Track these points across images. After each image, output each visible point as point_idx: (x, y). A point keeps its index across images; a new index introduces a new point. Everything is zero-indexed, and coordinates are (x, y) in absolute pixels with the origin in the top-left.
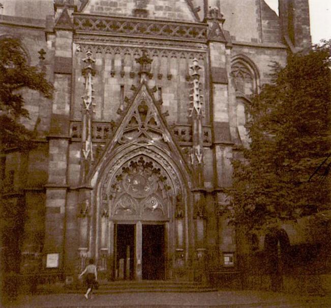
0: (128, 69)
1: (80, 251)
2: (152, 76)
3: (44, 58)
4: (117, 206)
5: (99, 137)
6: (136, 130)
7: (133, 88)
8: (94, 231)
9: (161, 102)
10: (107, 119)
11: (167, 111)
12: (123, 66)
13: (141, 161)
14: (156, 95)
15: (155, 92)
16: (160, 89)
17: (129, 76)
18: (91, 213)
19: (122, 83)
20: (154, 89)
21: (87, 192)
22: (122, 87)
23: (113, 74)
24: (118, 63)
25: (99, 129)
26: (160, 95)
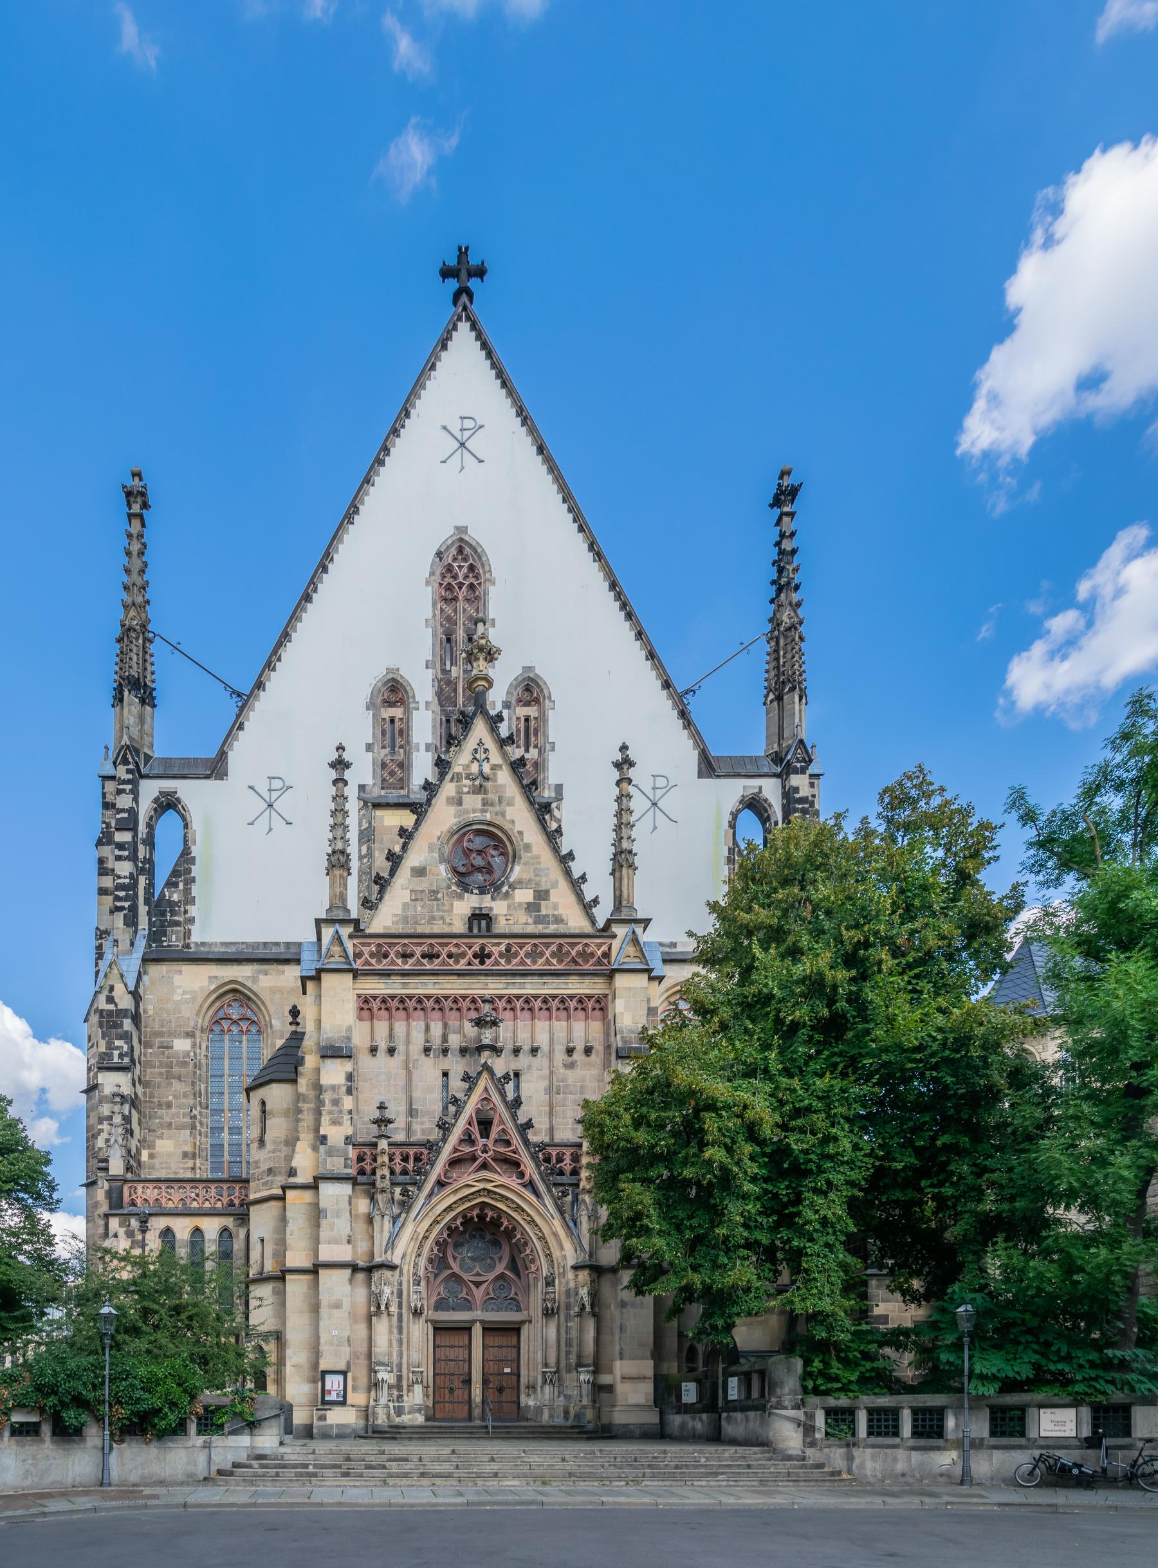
0: (455, 1041)
2: (501, 1051)
3: (298, 1024)
6: (474, 1158)
8: (400, 1342)
9: (517, 1102)
10: (418, 1137)
11: (530, 1120)
12: (445, 1038)
14: (510, 1087)
17: (457, 1052)
18: (394, 1309)
19: (446, 1067)
20: (506, 1077)
21: (387, 1273)
22: (445, 1074)
23: (427, 1050)
24: (437, 1029)
25: (405, 1159)
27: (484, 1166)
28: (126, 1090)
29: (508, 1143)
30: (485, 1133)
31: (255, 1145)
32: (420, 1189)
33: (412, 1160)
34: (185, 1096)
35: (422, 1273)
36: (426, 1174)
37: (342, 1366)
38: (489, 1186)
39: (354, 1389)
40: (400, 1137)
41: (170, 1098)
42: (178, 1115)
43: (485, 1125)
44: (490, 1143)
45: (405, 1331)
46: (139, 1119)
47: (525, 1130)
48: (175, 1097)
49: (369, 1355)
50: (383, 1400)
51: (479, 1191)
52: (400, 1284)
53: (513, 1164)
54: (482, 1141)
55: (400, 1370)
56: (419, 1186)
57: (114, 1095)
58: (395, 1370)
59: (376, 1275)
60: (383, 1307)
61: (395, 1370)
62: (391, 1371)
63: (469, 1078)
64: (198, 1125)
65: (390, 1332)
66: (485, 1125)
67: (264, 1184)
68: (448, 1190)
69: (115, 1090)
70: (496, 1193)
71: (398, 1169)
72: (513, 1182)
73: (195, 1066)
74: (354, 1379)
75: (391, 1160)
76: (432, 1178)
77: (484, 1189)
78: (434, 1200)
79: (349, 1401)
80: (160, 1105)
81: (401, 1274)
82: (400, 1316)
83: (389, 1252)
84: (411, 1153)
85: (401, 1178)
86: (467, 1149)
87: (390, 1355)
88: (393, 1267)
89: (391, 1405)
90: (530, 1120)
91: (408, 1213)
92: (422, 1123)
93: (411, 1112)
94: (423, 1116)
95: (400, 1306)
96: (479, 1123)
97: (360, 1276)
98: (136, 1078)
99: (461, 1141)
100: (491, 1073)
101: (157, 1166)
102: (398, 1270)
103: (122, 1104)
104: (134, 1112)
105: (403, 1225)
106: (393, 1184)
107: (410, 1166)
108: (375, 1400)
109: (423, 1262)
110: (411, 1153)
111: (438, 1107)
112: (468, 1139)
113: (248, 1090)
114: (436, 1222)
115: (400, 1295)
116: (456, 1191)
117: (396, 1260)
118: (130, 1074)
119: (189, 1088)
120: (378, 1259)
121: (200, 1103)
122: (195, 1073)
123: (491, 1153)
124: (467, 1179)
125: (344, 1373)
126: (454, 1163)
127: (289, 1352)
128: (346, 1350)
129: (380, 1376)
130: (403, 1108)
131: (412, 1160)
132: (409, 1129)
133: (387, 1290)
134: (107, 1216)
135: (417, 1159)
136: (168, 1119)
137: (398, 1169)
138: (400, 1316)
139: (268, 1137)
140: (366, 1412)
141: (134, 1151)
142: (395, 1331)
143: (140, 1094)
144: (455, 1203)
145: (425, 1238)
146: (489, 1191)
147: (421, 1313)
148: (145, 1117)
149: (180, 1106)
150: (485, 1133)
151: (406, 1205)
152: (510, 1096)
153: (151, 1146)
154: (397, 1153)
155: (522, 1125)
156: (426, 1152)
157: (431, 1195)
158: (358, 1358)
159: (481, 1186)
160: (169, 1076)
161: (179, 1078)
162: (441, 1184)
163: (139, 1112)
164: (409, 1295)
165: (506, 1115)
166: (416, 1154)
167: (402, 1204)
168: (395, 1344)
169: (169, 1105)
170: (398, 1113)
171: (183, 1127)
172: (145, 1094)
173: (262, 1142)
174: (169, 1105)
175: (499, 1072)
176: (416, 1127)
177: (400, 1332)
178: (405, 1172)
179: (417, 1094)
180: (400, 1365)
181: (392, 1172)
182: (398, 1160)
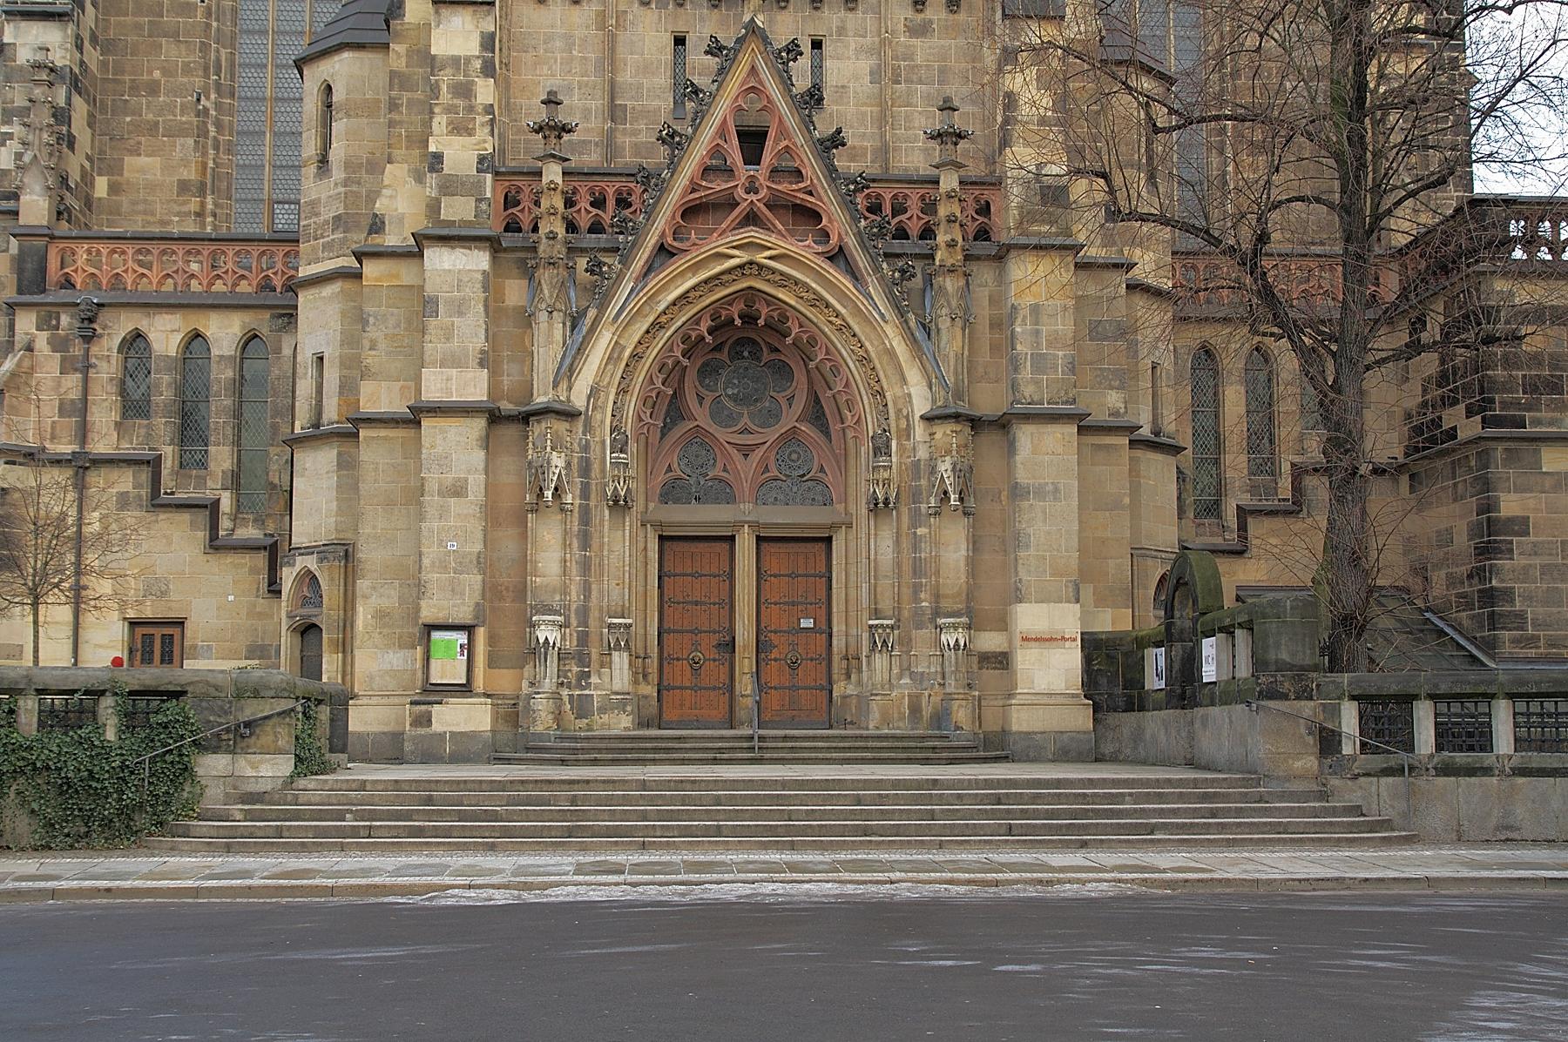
1: (533, 626)
4: (669, 469)
5: (596, 228)
7: (715, 49)
8: (585, 566)
9: (814, 98)
10: (627, 160)
13: (749, 319)
15: (795, 60)
16: (817, 45)
19: (681, 27)
20: (793, 50)
21: (561, 426)
22: (680, 41)
25: (599, 203)
26: (817, 68)
27: (751, 219)
28: (61, 57)
29: (798, 174)
30: (752, 157)
31: (312, 169)
32: (626, 262)
33: (611, 203)
34: (187, 70)
35: (629, 426)
36: (638, 232)
37: (464, 615)
38: (761, 257)
39: (492, 663)
40: (592, 159)
41: (157, 74)
42: (171, 108)
43: (752, 140)
44: (761, 172)
45: (595, 543)
46: (91, 116)
47: (827, 150)
48: (165, 72)
49: (521, 591)
50: (548, 684)
51: (741, 267)
52: (586, 448)
53: (805, 216)
54: (743, 172)
55: (584, 622)
56: (625, 255)
57: (38, 66)
58: (574, 622)
59: (537, 429)
60: (549, 494)
61: (574, 622)
62: (566, 625)
63: (721, 48)
64: (212, 128)
65: (565, 545)
66: (752, 140)
67: (328, 247)
68: (680, 263)
69: (40, 57)
70: (774, 271)
71: (584, 222)
72: (805, 249)
73: (209, 14)
74: (492, 640)
75: (569, 203)
76: (651, 241)
77: (751, 263)
78: (654, 282)
79: (479, 684)
80: (134, 89)
81: (588, 428)
82: (585, 514)
83: (564, 385)
84: (611, 191)
85: (591, 240)
86: (719, 185)
87: (565, 591)
88: (570, 415)
89: (565, 692)
90: (839, 131)
91: (602, 308)
92: (635, 133)
93: (615, 112)
94: (635, 120)
95: (585, 493)
96: (741, 135)
97: (510, 432)
98: (86, 36)
99: (707, 171)
100: (766, 41)
101: (125, 207)
102: (583, 416)
103: (51, 84)
104: (77, 100)
105: (592, 329)
106: (572, 250)
107: (606, 217)
108: (532, 684)
109: (631, 405)
110: (611, 191)
111: (665, 103)
112: (715, 168)
113: (300, 64)
114: (657, 326)
115: (585, 470)
116: (696, 267)
117: (579, 400)
118: (70, 30)
119: (195, 57)
120: (540, 399)
121: (218, 85)
122: (208, 26)
123: (763, 193)
124: (718, 244)
125: (469, 629)
126: (691, 212)
127: (362, 585)
128: (473, 581)
129: (542, 634)
130: (597, 103)
131: (611, 203)
132: (610, 145)
133: (558, 461)
134: (12, 307)
135: (623, 203)
136: (150, 116)
137: (584, 222)
138: (585, 514)
139: (337, 153)
140: (512, 713)
141: (75, 177)
142: (575, 544)
143: (93, 67)
144: (694, 288)
145: (636, 356)
146: (761, 267)
147: (627, 507)
148: (103, 110)
149: (175, 92)
150: (752, 157)
151: (600, 293)
152: (802, 83)
153: (114, 169)
154: (583, 190)
155: (821, 142)
156: (639, 189)
157: (649, 270)
158: (502, 598)
159: (741, 257)
160: (157, 30)
161: (175, 35)
162: (664, 252)
163: (92, 101)
164: (603, 471)
165: (791, 121)
166: (619, 192)
167: (592, 289)
168: (574, 569)
169: (153, 88)
170: (586, 113)
171: (183, 132)
172: (104, 65)
173: (323, 161)
174: (153, 88)
175: (781, 40)
176: (625, 141)
177: (585, 544)
178: (596, 228)
179: (626, 77)
180: (584, 613)
181: (571, 227)
182: (584, 204)
